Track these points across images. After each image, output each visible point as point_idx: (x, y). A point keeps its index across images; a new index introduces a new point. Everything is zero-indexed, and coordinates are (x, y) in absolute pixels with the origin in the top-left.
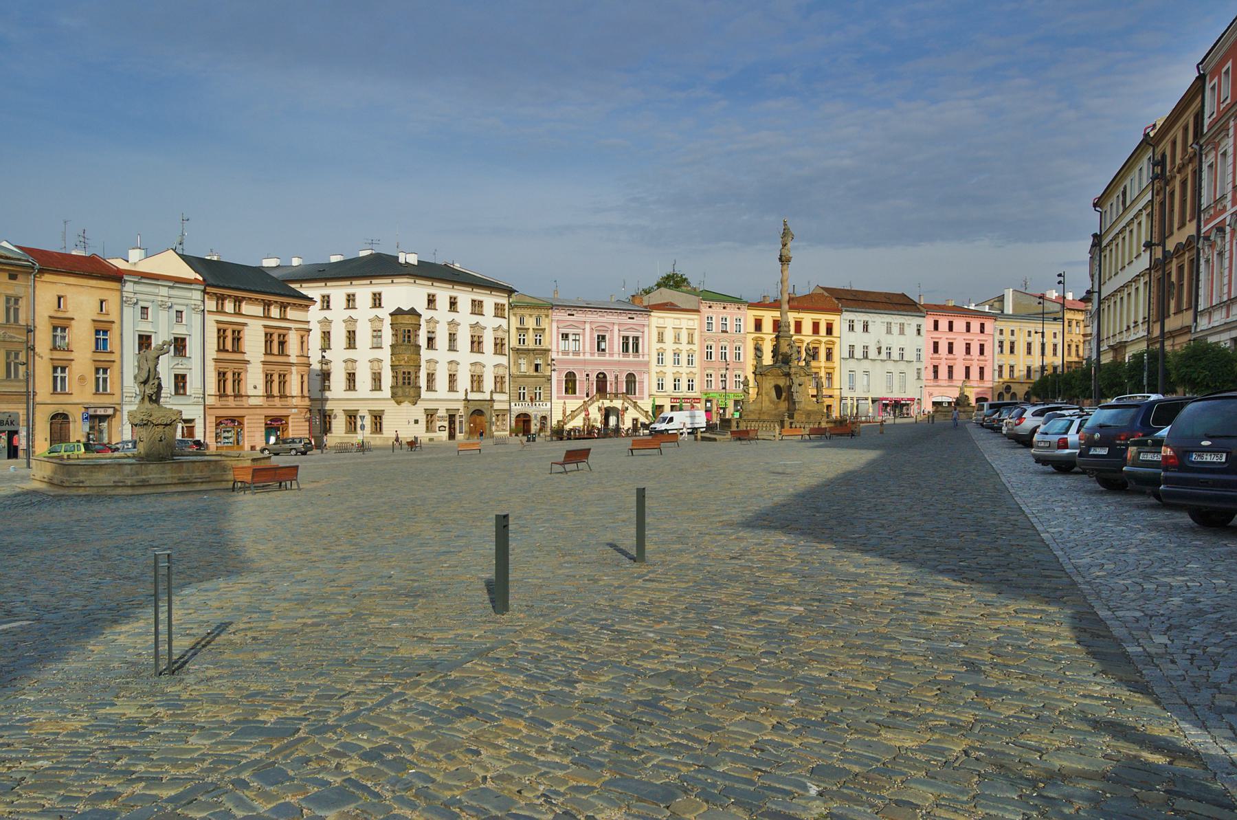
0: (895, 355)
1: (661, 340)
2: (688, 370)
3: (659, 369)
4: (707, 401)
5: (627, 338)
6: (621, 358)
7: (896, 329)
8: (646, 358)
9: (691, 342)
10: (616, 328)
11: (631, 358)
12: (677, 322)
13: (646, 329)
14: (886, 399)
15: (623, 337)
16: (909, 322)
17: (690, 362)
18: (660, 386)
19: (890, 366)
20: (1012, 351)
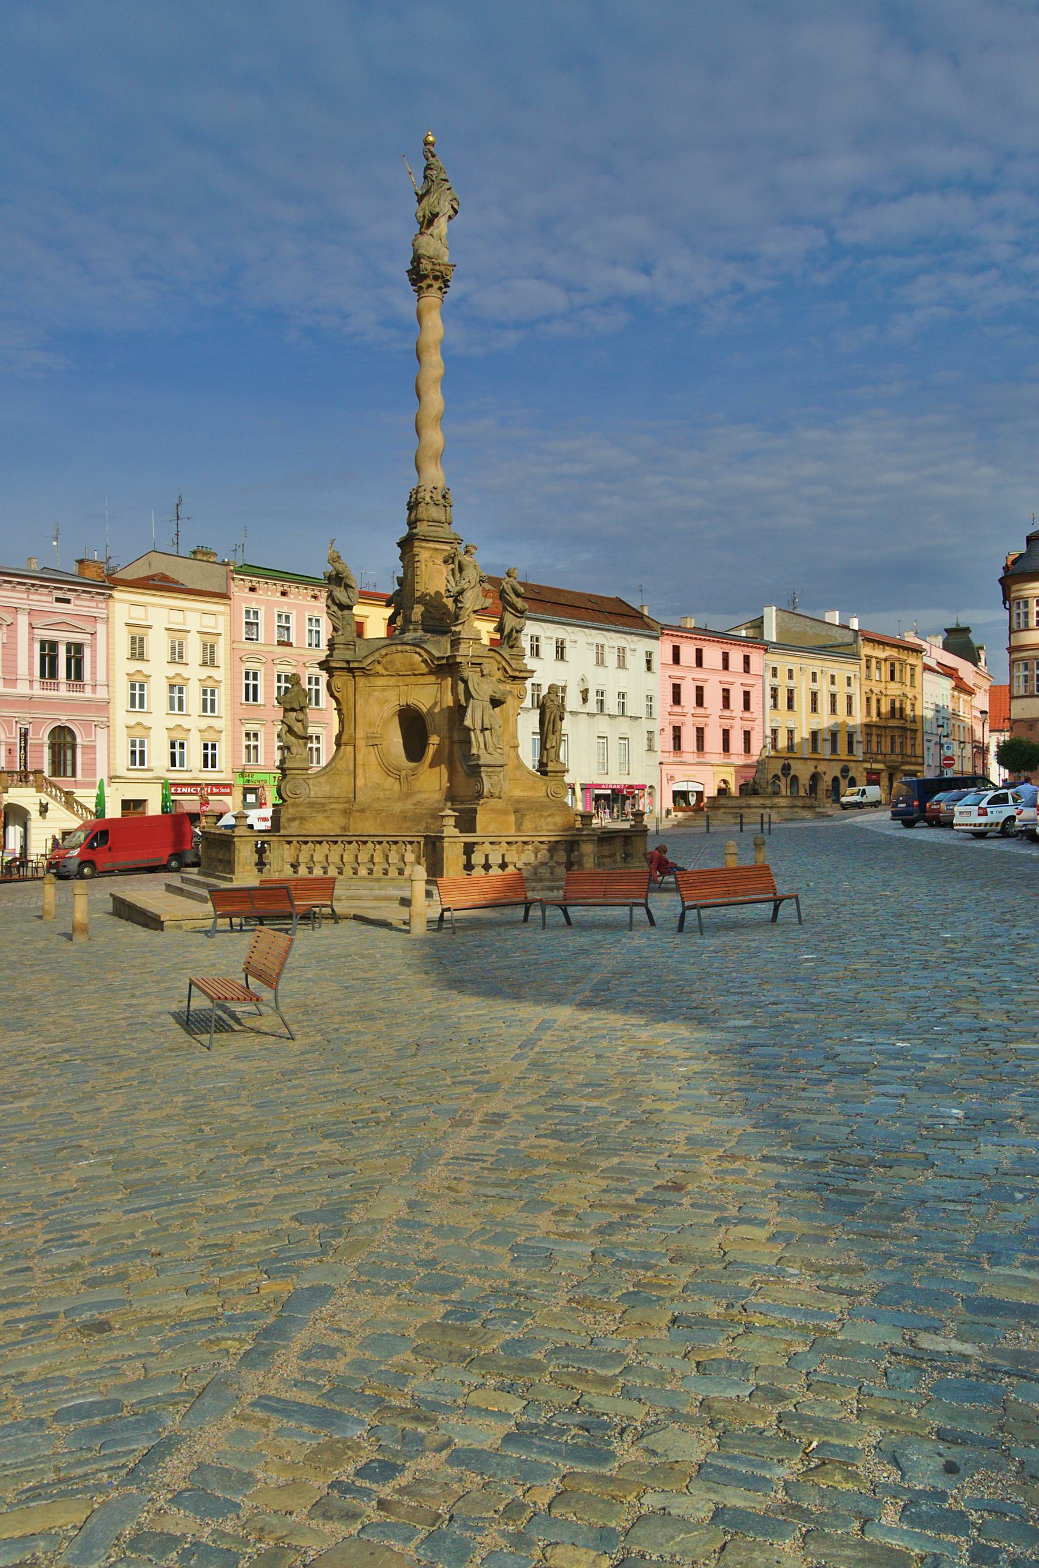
0: (612, 705)
1: (138, 651)
2: (204, 723)
3: (133, 719)
4: (247, 791)
5: (54, 645)
6: (37, 691)
7: (611, 658)
8: (101, 693)
9: (209, 660)
10: (23, 621)
11: (63, 692)
12: (177, 616)
13: (101, 628)
14: (599, 787)
15: (43, 643)
16: (633, 646)
17: (208, 706)
18: (137, 757)
19: (602, 725)
20: (790, 707)
